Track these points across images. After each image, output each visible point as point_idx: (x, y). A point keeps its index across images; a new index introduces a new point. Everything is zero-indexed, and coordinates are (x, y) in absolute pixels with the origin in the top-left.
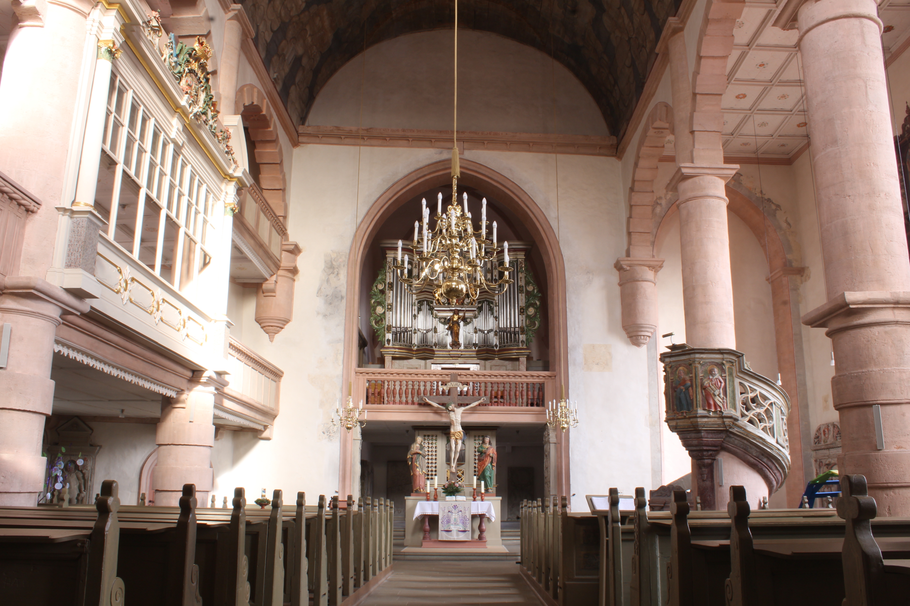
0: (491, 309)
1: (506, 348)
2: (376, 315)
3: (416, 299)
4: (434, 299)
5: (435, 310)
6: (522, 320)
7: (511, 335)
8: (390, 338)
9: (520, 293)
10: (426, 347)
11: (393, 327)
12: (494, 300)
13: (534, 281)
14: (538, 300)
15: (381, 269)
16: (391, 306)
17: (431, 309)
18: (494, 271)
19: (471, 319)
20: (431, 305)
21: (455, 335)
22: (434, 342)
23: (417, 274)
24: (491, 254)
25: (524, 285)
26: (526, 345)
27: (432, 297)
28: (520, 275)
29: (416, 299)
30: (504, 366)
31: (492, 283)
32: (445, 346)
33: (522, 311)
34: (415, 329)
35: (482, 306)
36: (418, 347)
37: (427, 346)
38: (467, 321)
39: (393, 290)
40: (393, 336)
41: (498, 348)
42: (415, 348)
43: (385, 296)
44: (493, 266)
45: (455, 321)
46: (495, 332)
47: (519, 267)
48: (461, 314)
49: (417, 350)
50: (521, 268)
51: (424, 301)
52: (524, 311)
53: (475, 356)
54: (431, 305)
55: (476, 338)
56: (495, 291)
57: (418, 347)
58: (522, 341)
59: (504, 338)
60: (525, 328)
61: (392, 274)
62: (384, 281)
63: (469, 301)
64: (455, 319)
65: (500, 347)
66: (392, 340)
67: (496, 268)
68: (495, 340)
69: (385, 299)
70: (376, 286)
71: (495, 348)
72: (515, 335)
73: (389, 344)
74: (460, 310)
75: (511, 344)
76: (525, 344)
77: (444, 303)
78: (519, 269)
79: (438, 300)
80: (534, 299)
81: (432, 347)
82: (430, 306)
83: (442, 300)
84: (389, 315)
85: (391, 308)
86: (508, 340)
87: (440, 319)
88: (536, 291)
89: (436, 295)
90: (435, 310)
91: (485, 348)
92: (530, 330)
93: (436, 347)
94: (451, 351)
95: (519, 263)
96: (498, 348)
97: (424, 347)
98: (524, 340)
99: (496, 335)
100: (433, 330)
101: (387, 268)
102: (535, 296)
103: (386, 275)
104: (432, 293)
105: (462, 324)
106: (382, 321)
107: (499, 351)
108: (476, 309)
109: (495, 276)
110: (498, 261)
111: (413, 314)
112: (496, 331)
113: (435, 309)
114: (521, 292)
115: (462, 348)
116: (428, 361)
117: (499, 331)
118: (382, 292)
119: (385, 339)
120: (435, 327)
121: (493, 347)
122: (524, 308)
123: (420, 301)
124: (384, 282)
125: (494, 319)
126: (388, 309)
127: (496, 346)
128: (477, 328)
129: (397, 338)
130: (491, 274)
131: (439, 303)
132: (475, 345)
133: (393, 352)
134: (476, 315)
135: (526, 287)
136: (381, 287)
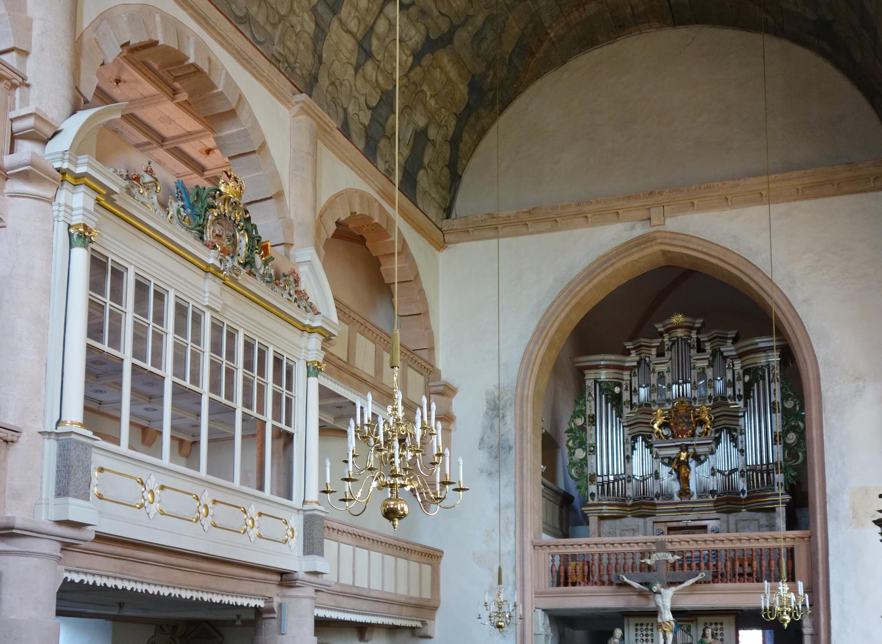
0: (734, 440)
1: (756, 494)
4: (653, 432)
8: (595, 491)
10: (644, 501)
11: (598, 476)
12: (738, 425)
16: (594, 447)
17: (649, 446)
18: (736, 383)
19: (705, 455)
20: (650, 440)
21: (684, 480)
22: (655, 492)
23: (629, 399)
24: (731, 359)
27: (649, 429)
30: (756, 520)
31: (735, 401)
35: (720, 437)
36: (634, 500)
37: (644, 498)
38: (700, 459)
39: (596, 426)
40: (598, 489)
41: (746, 495)
43: (586, 434)
44: (736, 376)
46: (741, 472)
48: (691, 450)
49: (632, 505)
51: (638, 436)
53: (713, 508)
54: (650, 440)
55: (714, 483)
56: (738, 412)
61: (593, 402)
64: (682, 459)
65: (748, 493)
66: (598, 494)
68: (741, 484)
69: (586, 438)
71: (742, 495)
72: (768, 475)
73: (593, 499)
75: (763, 488)
77: (667, 437)
81: (652, 499)
82: (648, 442)
83: (666, 432)
84: (591, 460)
85: (593, 451)
87: (663, 458)
92: (790, 465)
93: (658, 499)
95: (771, 368)
96: (746, 495)
99: (742, 476)
100: (654, 475)
101: (587, 396)
103: (585, 406)
104: (648, 423)
107: (747, 499)
109: (739, 390)
110: (742, 368)
111: (626, 455)
112: (742, 471)
113: (655, 446)
115: (694, 498)
117: (747, 470)
119: (588, 493)
120: (656, 471)
121: (738, 494)
125: (739, 453)
126: (591, 451)
127: (743, 491)
128: (715, 468)
129: (604, 490)
130: (732, 389)
132: (713, 492)
134: (712, 450)
135: (782, 402)
136: (579, 422)
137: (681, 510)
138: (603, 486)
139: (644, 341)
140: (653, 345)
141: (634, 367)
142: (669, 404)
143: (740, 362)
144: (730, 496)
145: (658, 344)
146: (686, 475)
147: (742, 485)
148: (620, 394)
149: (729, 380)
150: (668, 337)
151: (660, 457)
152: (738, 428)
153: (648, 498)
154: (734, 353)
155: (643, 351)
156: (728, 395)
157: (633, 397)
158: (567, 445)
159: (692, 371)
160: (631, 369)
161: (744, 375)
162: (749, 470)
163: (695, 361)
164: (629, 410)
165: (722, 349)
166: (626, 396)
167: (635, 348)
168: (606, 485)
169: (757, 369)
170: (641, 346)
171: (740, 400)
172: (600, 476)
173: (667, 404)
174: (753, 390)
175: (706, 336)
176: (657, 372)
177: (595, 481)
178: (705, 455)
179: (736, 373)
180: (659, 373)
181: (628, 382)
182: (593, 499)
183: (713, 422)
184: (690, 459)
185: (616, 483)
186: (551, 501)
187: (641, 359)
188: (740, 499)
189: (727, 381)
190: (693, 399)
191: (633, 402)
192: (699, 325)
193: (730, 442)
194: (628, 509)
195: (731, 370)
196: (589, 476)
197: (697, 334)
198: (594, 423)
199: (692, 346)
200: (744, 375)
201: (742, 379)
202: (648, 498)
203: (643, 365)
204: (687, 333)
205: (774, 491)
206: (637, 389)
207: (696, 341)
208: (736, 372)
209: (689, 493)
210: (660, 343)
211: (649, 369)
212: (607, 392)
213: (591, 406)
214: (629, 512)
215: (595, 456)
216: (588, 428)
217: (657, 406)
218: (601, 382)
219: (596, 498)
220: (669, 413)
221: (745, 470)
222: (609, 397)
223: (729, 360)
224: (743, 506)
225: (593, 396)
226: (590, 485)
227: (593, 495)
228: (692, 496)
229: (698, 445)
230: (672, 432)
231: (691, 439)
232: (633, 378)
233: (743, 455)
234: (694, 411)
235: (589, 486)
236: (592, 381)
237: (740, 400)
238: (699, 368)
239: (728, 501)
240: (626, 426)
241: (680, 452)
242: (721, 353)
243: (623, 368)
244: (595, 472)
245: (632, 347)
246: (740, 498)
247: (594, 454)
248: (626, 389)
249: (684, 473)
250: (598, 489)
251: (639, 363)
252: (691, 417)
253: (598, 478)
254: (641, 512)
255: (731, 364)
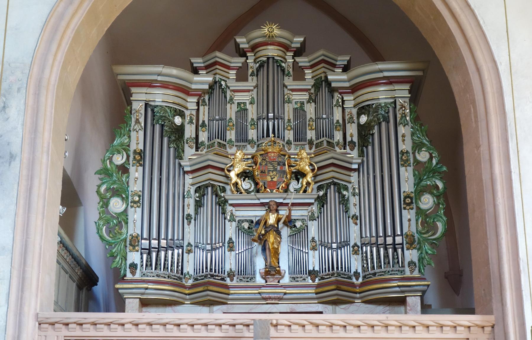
2: (109, 216)
3: (192, 185)
4: (227, 184)
5: (231, 205)
6: (409, 220)
7: (386, 249)
9: (403, 165)
10: (212, 280)
12: (350, 183)
13: (430, 142)
14: (441, 179)
15: (122, 125)
16: (139, 196)
20: (222, 194)
22: (227, 269)
23: (194, 136)
24: (340, 93)
25: (410, 151)
26: (420, 271)
28: (402, 130)
29: (192, 185)
32: (252, 278)
33: (408, 200)
34: (189, 244)
35: (326, 194)
36: (196, 279)
37: (212, 276)
38: (295, 226)
40: (142, 258)
41: (360, 280)
42: (190, 282)
45: (271, 225)
46: (353, 247)
47: (399, 116)
48: (283, 212)
49: (193, 286)
50: (404, 116)
52: (412, 202)
53: (314, 296)
54: (222, 194)
56: (351, 163)
57: (196, 279)
58: (411, 263)
59: (372, 259)
60: (416, 236)
61: (141, 133)
62: (126, 148)
63: (300, 185)
65: (364, 277)
67: (351, 121)
69: (128, 183)
70: (111, 159)
71: (354, 280)
72: (395, 250)
73: (133, 273)
74: (281, 204)
75: (388, 269)
76: (417, 269)
77: (248, 191)
78: (398, 119)
79: (236, 184)
80: (433, 177)
81: (223, 279)
82: (221, 197)
83: (246, 185)
85: (139, 201)
86: (380, 262)
88: (434, 162)
89: (233, 175)
90: (231, 205)
91: (333, 279)
93: (232, 280)
94: (263, 286)
95: (398, 107)
96: (360, 280)
97: (206, 280)
98: (416, 260)
100: (226, 245)
101: (133, 123)
102: (433, 172)
103: (129, 137)
104: (222, 170)
105: (285, 232)
106: (121, 228)
107: (362, 285)
108: (313, 201)
109: (352, 136)
111: (186, 213)
112: (355, 245)
113: (230, 202)
114: (406, 163)
115: (286, 280)
116: (216, 308)
117: (363, 244)
118: (124, 169)
119: (126, 264)
120: (230, 239)
121: (350, 278)
122: (413, 195)
123: (199, 187)
124: (124, 149)
126: (135, 202)
128: (316, 239)
129: (151, 261)
130: (341, 132)
131: (238, 190)
132: (313, 274)
133: (143, 291)
134: (313, 214)
135: (414, 153)
136: (119, 160)
137: (267, 296)
138: (149, 254)
139: (220, 56)
140: (232, 65)
141: (204, 92)
142: (253, 147)
143: (352, 98)
144: (339, 278)
145: (240, 65)
146: (276, 247)
147: (356, 264)
148: (182, 126)
149: (338, 121)
150: (254, 57)
151: (237, 219)
152: (350, 186)
153: (217, 276)
154: (347, 85)
155: (218, 71)
156: (336, 140)
157: (201, 133)
158: (98, 192)
159: (286, 105)
160: (199, 94)
161: (359, 115)
162: (366, 245)
163: (290, 92)
164: (193, 151)
165: (330, 77)
166: (189, 131)
167: (206, 68)
168: (154, 255)
169: (379, 106)
170: (216, 63)
171: (352, 149)
172: (145, 239)
173: (249, 146)
174: (373, 135)
175: (307, 60)
176: (236, 102)
177: (138, 245)
178: (303, 220)
179: (347, 113)
180: (239, 104)
181: (194, 113)
182: (133, 273)
183: (315, 176)
184: (281, 225)
185: (170, 252)
186: (67, 273)
187: (215, 82)
188: (353, 285)
189: (335, 121)
190: (287, 143)
191: (200, 141)
192: (299, 45)
193: (339, 204)
194: (187, 292)
195: (340, 109)
196: (129, 238)
197: (293, 57)
198: (142, 162)
199: (286, 72)
200: (359, 115)
201: (356, 121)
202: (217, 276)
203: (217, 91)
204: (281, 53)
205: (404, 274)
206: (207, 123)
207: (291, 66)
208: (347, 111)
209: (279, 272)
210: (242, 63)
211: (225, 97)
212: (163, 120)
213: (138, 137)
214: (188, 297)
215: (141, 209)
216: (132, 169)
217: (235, 148)
218: (156, 106)
219: (138, 271)
220: (253, 158)
221: (359, 244)
222: (166, 128)
223: (337, 95)
224: (358, 295)
225: (143, 125)
226: (130, 251)
227: (133, 266)
228: (283, 277)
229: (293, 204)
230: (256, 184)
231: (285, 195)
232: (201, 108)
233: (356, 224)
234: (289, 157)
235: (129, 254)
236: (143, 104)
237: (352, 149)
238: (296, 103)
239: (339, 285)
240: (188, 172)
241: (267, 214)
242: (328, 83)
243: (187, 91)
244: (140, 234)
245: (202, 65)
246: (353, 283)
247: (138, 207)
248: (191, 122)
249: (273, 244)
250: (142, 258)
251: (211, 87)
252: (284, 165)
253: (143, 241)
254: (208, 295)
255: (340, 100)
